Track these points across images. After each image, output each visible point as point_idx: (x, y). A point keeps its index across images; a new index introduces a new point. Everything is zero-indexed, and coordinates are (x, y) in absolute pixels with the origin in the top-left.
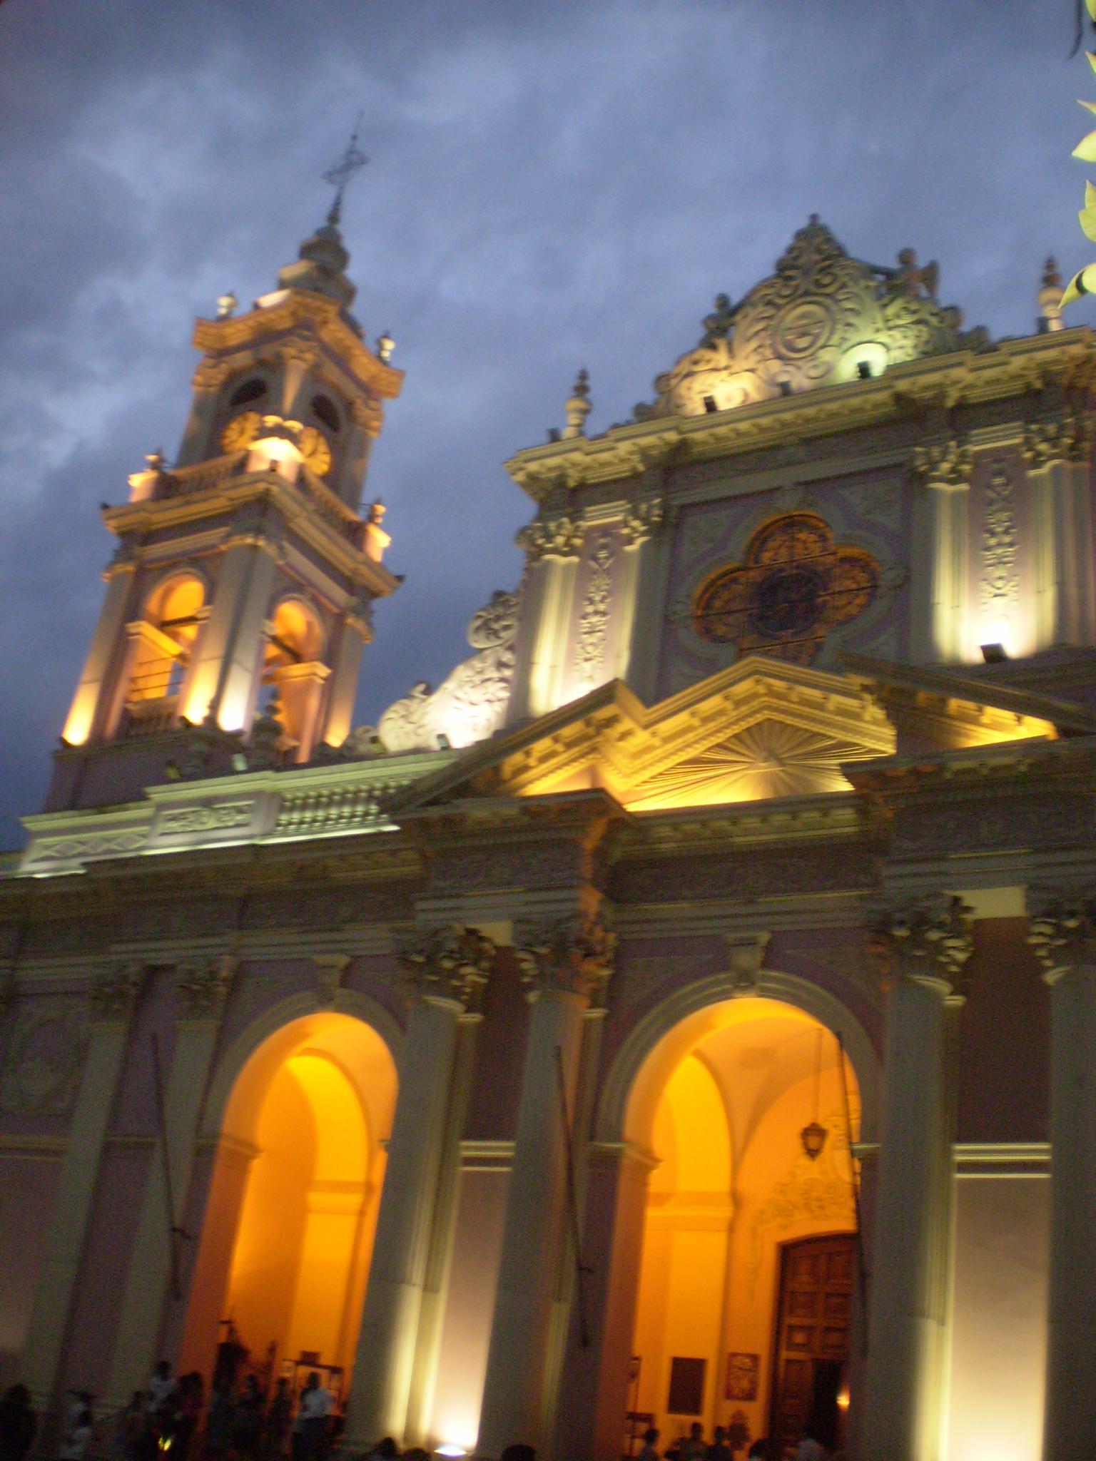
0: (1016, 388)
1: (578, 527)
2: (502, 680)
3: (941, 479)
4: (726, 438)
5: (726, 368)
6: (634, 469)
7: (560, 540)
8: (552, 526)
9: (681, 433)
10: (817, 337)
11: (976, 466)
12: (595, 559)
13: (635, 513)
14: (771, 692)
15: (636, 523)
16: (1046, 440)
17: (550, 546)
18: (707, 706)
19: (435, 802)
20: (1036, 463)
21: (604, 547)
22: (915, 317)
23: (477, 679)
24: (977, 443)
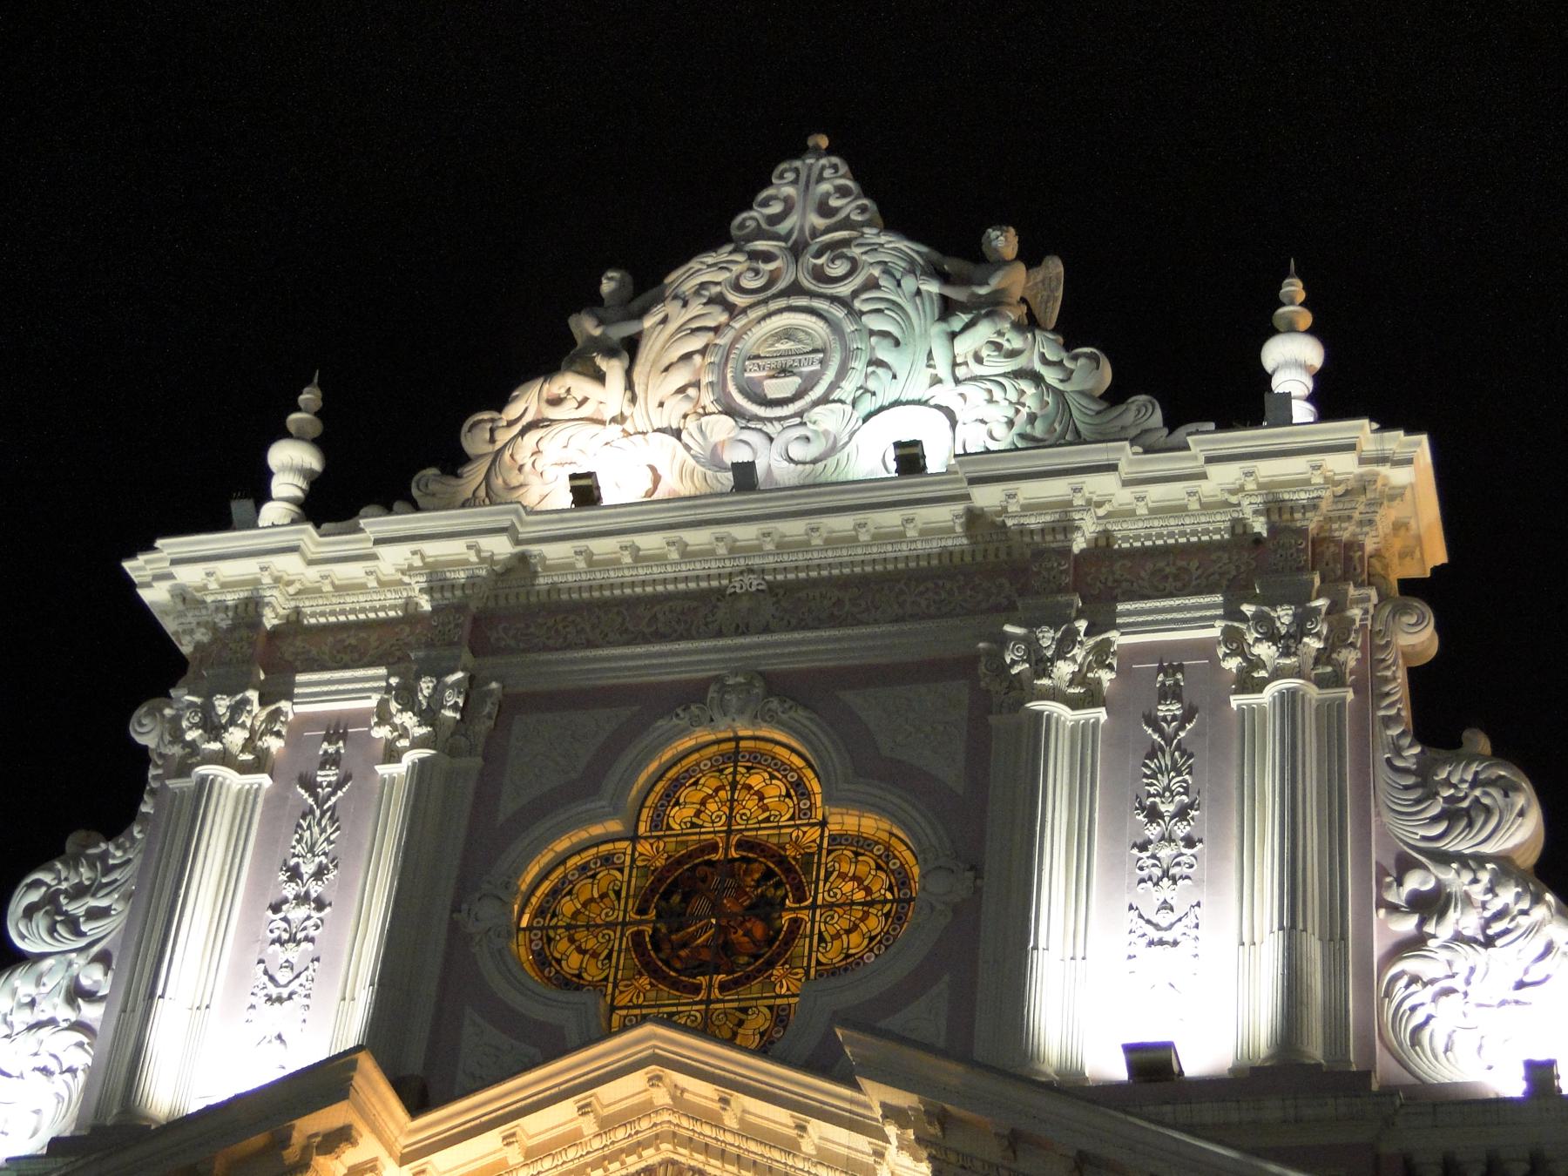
0: (1216, 527)
1: (278, 712)
2: (79, 1026)
3: (1055, 695)
4: (614, 563)
5: (620, 419)
6: (409, 603)
7: (235, 737)
8: (222, 704)
9: (518, 542)
10: (810, 382)
11: (1123, 672)
12: (310, 786)
13: (407, 698)
14: (680, 1104)
15: (408, 719)
16: (1272, 636)
17: (216, 746)
18: (537, 1126)
20: (1248, 683)
21: (331, 760)
23: (24, 1018)
24: (1126, 629)
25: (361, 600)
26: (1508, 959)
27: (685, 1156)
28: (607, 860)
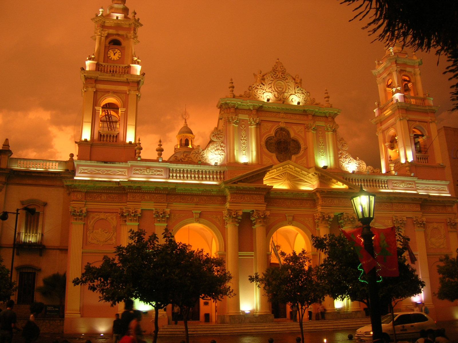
2: (222, 150)
19: (235, 183)
21: (243, 124)
22: (302, 92)
25: (245, 107)
26: (348, 160)
27: (288, 172)
28: (271, 139)
